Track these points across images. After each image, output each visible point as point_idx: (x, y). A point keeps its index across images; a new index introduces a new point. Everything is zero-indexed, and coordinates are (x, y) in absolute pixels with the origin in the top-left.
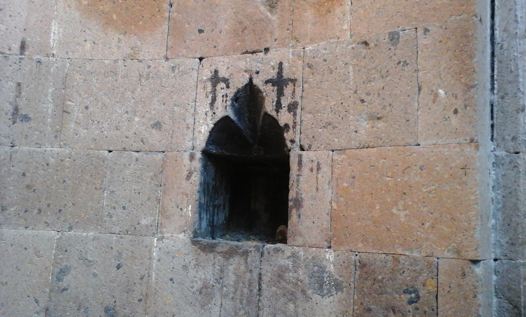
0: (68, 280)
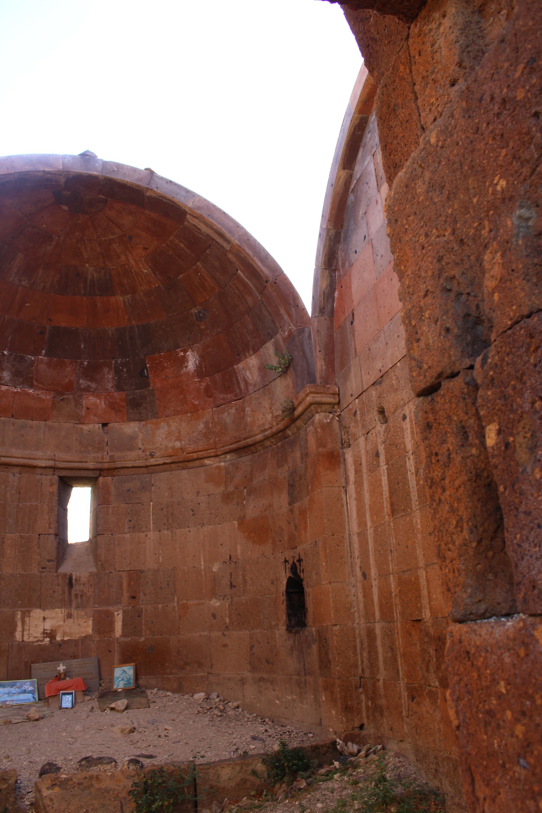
0: (254, 649)
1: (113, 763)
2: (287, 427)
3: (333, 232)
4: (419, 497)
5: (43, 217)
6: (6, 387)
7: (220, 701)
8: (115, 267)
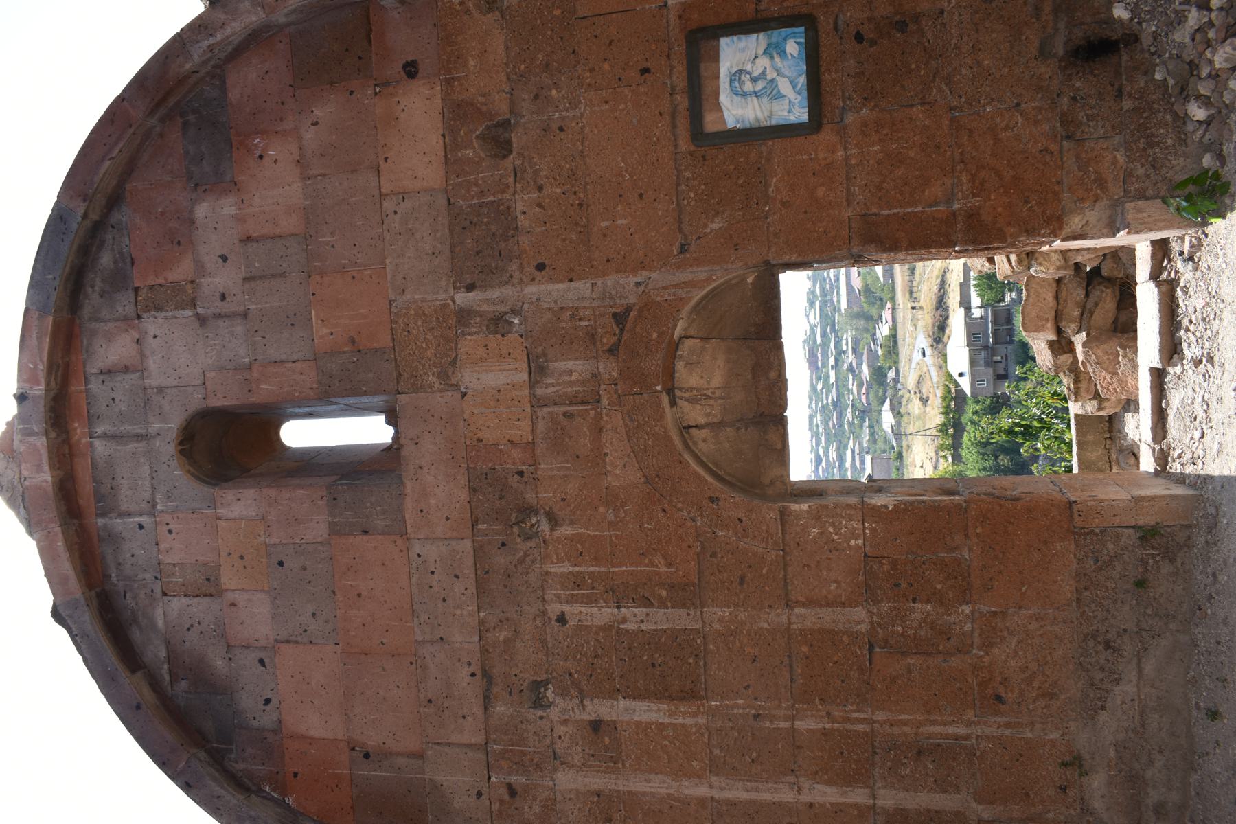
4: (684, 606)
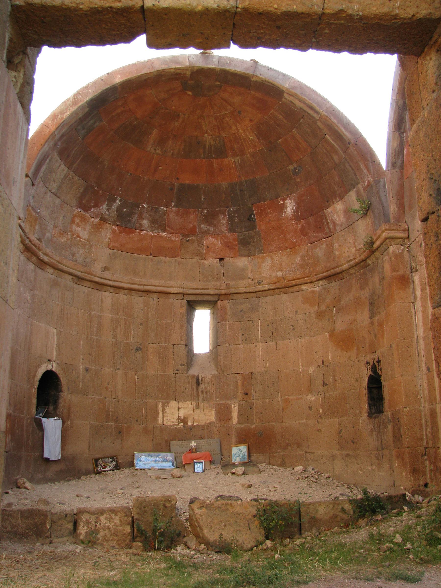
0: (342, 432)
1: (240, 500)
2: (368, 257)
3: (401, 102)
5: (173, 101)
6: (145, 232)
7: (315, 472)
8: (227, 135)
